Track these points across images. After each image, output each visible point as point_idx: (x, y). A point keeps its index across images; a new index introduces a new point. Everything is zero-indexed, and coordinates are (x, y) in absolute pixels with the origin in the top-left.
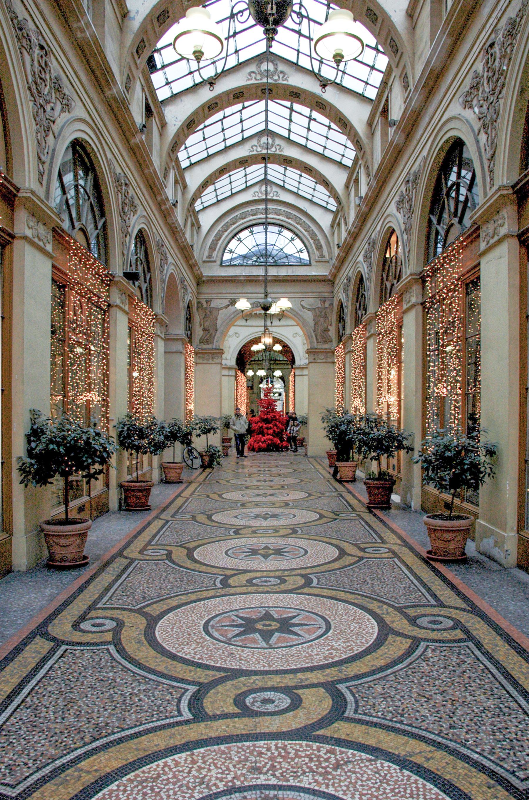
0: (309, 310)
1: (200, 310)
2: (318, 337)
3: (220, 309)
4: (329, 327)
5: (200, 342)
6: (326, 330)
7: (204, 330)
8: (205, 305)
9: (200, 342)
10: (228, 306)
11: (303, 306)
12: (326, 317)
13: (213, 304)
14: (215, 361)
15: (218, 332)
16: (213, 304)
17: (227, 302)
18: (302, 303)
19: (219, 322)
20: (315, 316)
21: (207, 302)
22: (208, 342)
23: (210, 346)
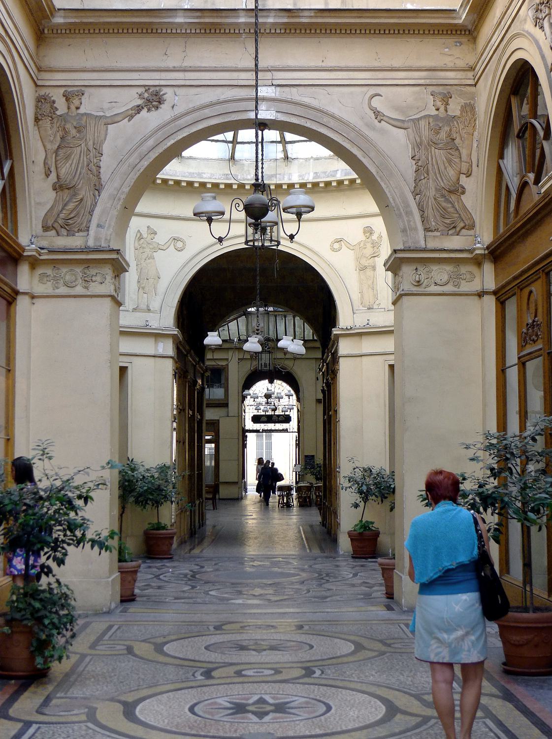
0: (399, 125)
1: (46, 123)
2: (430, 212)
3: (114, 120)
4: (463, 180)
5: (46, 228)
6: (457, 190)
7: (58, 187)
8: (61, 106)
9: (46, 228)
10: (139, 109)
11: (377, 113)
12: (451, 145)
13: (88, 106)
14: (95, 288)
15: (104, 194)
16: (88, 106)
17: (131, 98)
18: (376, 103)
19: (107, 164)
20: (418, 145)
21: (67, 97)
22: (68, 226)
23: (76, 241)
